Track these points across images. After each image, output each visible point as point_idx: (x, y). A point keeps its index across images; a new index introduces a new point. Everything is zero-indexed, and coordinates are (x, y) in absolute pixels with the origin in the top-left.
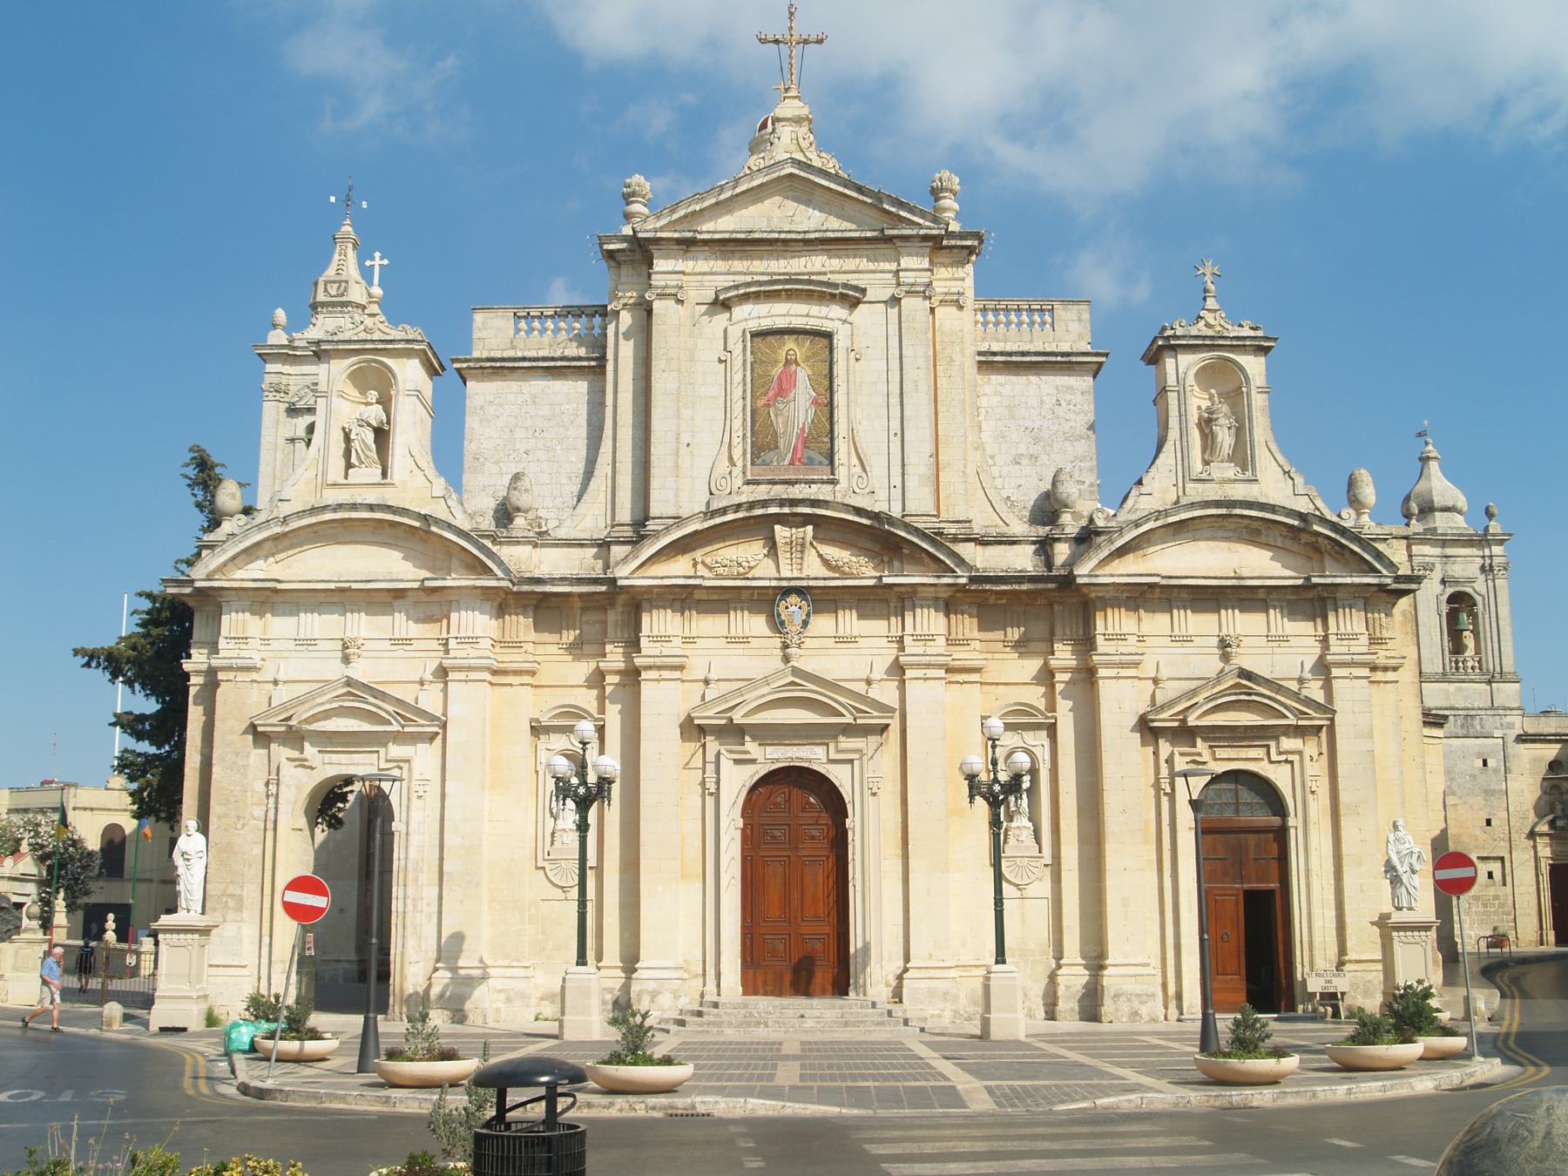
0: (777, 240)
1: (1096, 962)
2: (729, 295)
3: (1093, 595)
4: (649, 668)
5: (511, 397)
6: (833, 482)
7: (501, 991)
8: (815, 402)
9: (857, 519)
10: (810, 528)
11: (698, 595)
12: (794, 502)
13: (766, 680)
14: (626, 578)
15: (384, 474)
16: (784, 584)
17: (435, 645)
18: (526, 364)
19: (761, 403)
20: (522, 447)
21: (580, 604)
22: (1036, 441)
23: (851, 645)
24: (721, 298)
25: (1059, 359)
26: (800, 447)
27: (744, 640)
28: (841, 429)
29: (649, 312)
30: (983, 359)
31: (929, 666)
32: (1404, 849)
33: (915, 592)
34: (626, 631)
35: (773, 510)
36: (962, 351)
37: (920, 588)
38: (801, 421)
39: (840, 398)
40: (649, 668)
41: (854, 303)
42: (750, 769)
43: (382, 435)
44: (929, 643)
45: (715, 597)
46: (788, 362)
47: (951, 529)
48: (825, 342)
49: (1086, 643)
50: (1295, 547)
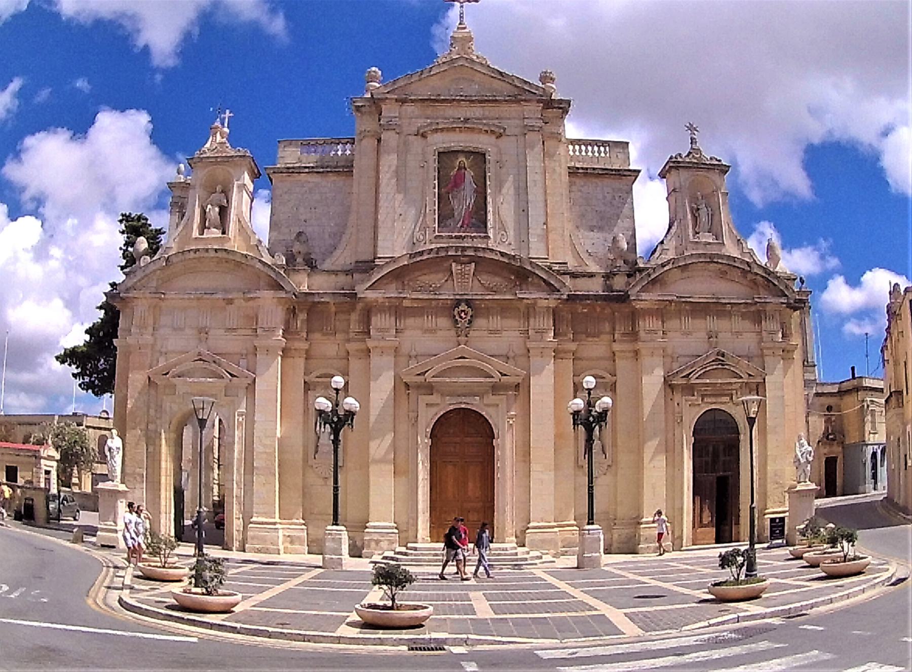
0: (454, 100)
1: (635, 520)
2: (426, 129)
3: (638, 307)
5: (298, 189)
6: (488, 237)
7: (289, 536)
8: (476, 191)
9: (501, 259)
10: (473, 264)
11: (406, 303)
12: (464, 249)
15: (224, 233)
16: (458, 297)
17: (249, 332)
18: (307, 170)
20: (303, 217)
21: (333, 309)
22: (602, 219)
24: (421, 131)
25: (614, 172)
26: (466, 216)
27: (432, 331)
29: (379, 141)
32: (803, 450)
33: (535, 304)
34: (361, 324)
36: (560, 166)
37: (539, 301)
41: (500, 135)
42: (433, 410)
43: (224, 211)
46: (460, 168)
47: (556, 267)
48: (481, 157)
49: (634, 335)
50: (745, 282)
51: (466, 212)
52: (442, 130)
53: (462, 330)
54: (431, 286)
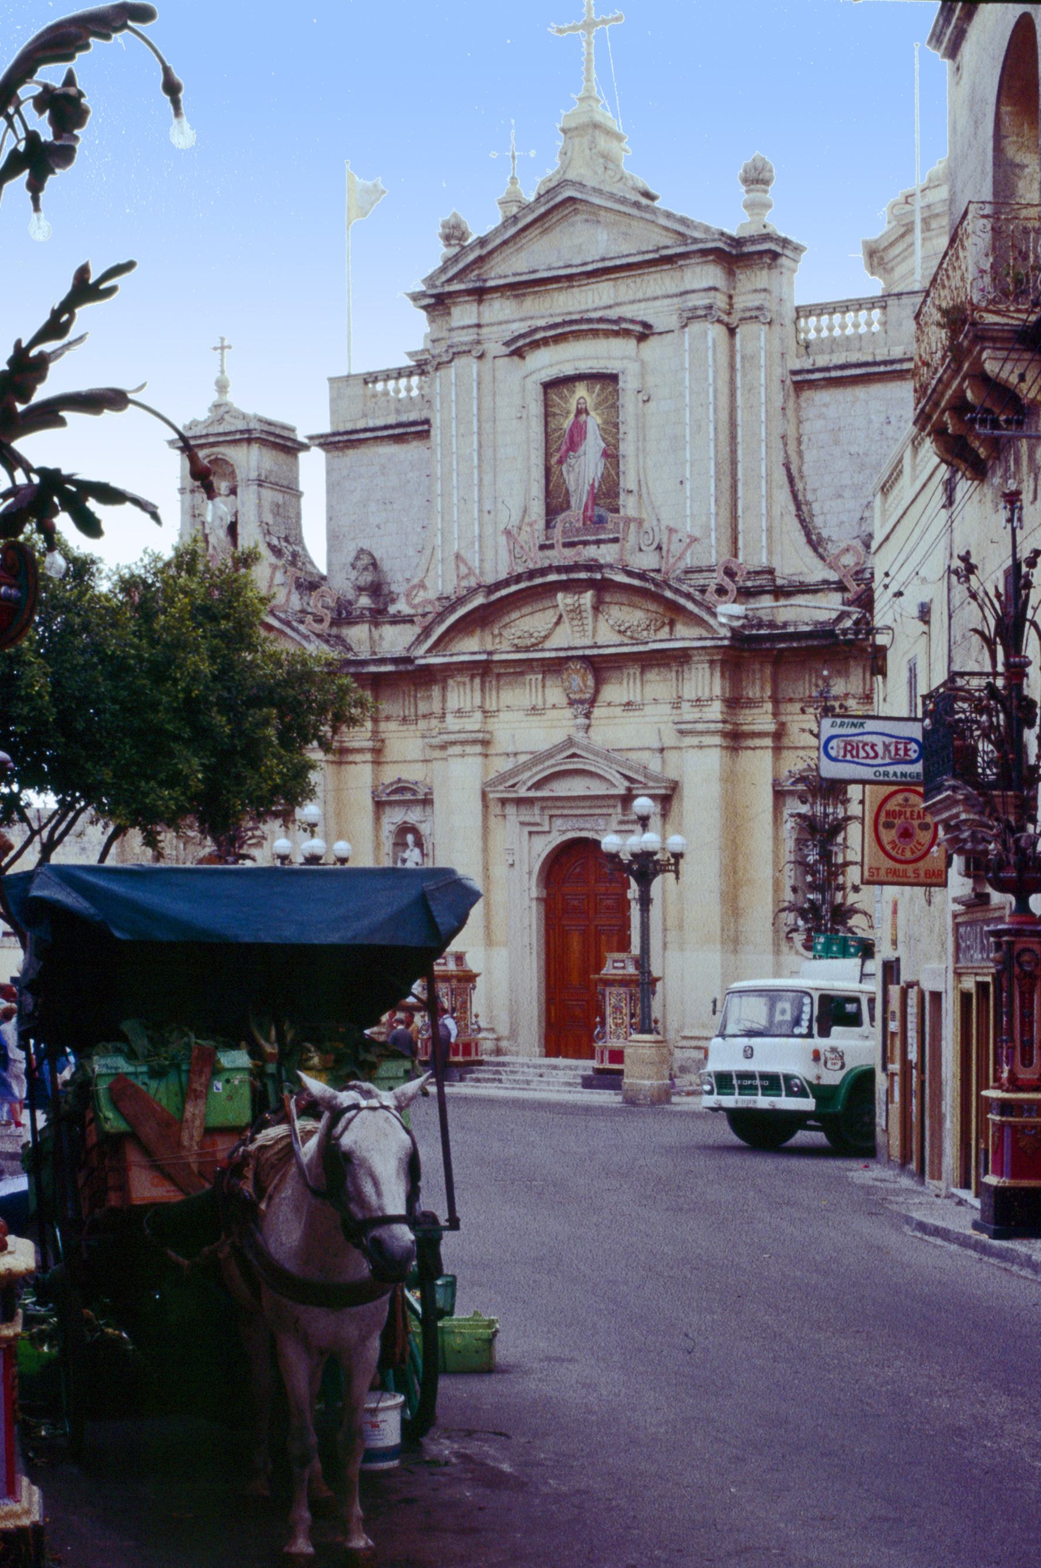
4: (453, 743)
8: (605, 454)
13: (549, 754)
14: (425, 657)
19: (554, 460)
23: (637, 713)
26: (590, 503)
28: (628, 481)
30: (799, 378)
31: (701, 733)
35: (552, 577)
38: (592, 475)
39: (627, 447)
40: (453, 743)
41: (642, 338)
44: (705, 709)
45: (512, 670)
46: (579, 412)
51: (588, 493)
52: (545, 342)
53: (584, 706)
54: (531, 636)
